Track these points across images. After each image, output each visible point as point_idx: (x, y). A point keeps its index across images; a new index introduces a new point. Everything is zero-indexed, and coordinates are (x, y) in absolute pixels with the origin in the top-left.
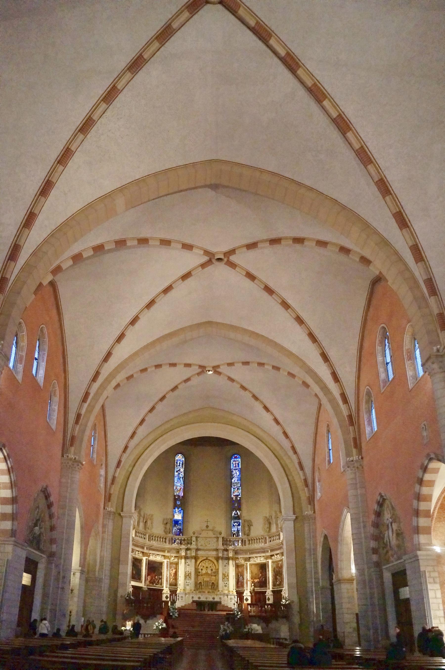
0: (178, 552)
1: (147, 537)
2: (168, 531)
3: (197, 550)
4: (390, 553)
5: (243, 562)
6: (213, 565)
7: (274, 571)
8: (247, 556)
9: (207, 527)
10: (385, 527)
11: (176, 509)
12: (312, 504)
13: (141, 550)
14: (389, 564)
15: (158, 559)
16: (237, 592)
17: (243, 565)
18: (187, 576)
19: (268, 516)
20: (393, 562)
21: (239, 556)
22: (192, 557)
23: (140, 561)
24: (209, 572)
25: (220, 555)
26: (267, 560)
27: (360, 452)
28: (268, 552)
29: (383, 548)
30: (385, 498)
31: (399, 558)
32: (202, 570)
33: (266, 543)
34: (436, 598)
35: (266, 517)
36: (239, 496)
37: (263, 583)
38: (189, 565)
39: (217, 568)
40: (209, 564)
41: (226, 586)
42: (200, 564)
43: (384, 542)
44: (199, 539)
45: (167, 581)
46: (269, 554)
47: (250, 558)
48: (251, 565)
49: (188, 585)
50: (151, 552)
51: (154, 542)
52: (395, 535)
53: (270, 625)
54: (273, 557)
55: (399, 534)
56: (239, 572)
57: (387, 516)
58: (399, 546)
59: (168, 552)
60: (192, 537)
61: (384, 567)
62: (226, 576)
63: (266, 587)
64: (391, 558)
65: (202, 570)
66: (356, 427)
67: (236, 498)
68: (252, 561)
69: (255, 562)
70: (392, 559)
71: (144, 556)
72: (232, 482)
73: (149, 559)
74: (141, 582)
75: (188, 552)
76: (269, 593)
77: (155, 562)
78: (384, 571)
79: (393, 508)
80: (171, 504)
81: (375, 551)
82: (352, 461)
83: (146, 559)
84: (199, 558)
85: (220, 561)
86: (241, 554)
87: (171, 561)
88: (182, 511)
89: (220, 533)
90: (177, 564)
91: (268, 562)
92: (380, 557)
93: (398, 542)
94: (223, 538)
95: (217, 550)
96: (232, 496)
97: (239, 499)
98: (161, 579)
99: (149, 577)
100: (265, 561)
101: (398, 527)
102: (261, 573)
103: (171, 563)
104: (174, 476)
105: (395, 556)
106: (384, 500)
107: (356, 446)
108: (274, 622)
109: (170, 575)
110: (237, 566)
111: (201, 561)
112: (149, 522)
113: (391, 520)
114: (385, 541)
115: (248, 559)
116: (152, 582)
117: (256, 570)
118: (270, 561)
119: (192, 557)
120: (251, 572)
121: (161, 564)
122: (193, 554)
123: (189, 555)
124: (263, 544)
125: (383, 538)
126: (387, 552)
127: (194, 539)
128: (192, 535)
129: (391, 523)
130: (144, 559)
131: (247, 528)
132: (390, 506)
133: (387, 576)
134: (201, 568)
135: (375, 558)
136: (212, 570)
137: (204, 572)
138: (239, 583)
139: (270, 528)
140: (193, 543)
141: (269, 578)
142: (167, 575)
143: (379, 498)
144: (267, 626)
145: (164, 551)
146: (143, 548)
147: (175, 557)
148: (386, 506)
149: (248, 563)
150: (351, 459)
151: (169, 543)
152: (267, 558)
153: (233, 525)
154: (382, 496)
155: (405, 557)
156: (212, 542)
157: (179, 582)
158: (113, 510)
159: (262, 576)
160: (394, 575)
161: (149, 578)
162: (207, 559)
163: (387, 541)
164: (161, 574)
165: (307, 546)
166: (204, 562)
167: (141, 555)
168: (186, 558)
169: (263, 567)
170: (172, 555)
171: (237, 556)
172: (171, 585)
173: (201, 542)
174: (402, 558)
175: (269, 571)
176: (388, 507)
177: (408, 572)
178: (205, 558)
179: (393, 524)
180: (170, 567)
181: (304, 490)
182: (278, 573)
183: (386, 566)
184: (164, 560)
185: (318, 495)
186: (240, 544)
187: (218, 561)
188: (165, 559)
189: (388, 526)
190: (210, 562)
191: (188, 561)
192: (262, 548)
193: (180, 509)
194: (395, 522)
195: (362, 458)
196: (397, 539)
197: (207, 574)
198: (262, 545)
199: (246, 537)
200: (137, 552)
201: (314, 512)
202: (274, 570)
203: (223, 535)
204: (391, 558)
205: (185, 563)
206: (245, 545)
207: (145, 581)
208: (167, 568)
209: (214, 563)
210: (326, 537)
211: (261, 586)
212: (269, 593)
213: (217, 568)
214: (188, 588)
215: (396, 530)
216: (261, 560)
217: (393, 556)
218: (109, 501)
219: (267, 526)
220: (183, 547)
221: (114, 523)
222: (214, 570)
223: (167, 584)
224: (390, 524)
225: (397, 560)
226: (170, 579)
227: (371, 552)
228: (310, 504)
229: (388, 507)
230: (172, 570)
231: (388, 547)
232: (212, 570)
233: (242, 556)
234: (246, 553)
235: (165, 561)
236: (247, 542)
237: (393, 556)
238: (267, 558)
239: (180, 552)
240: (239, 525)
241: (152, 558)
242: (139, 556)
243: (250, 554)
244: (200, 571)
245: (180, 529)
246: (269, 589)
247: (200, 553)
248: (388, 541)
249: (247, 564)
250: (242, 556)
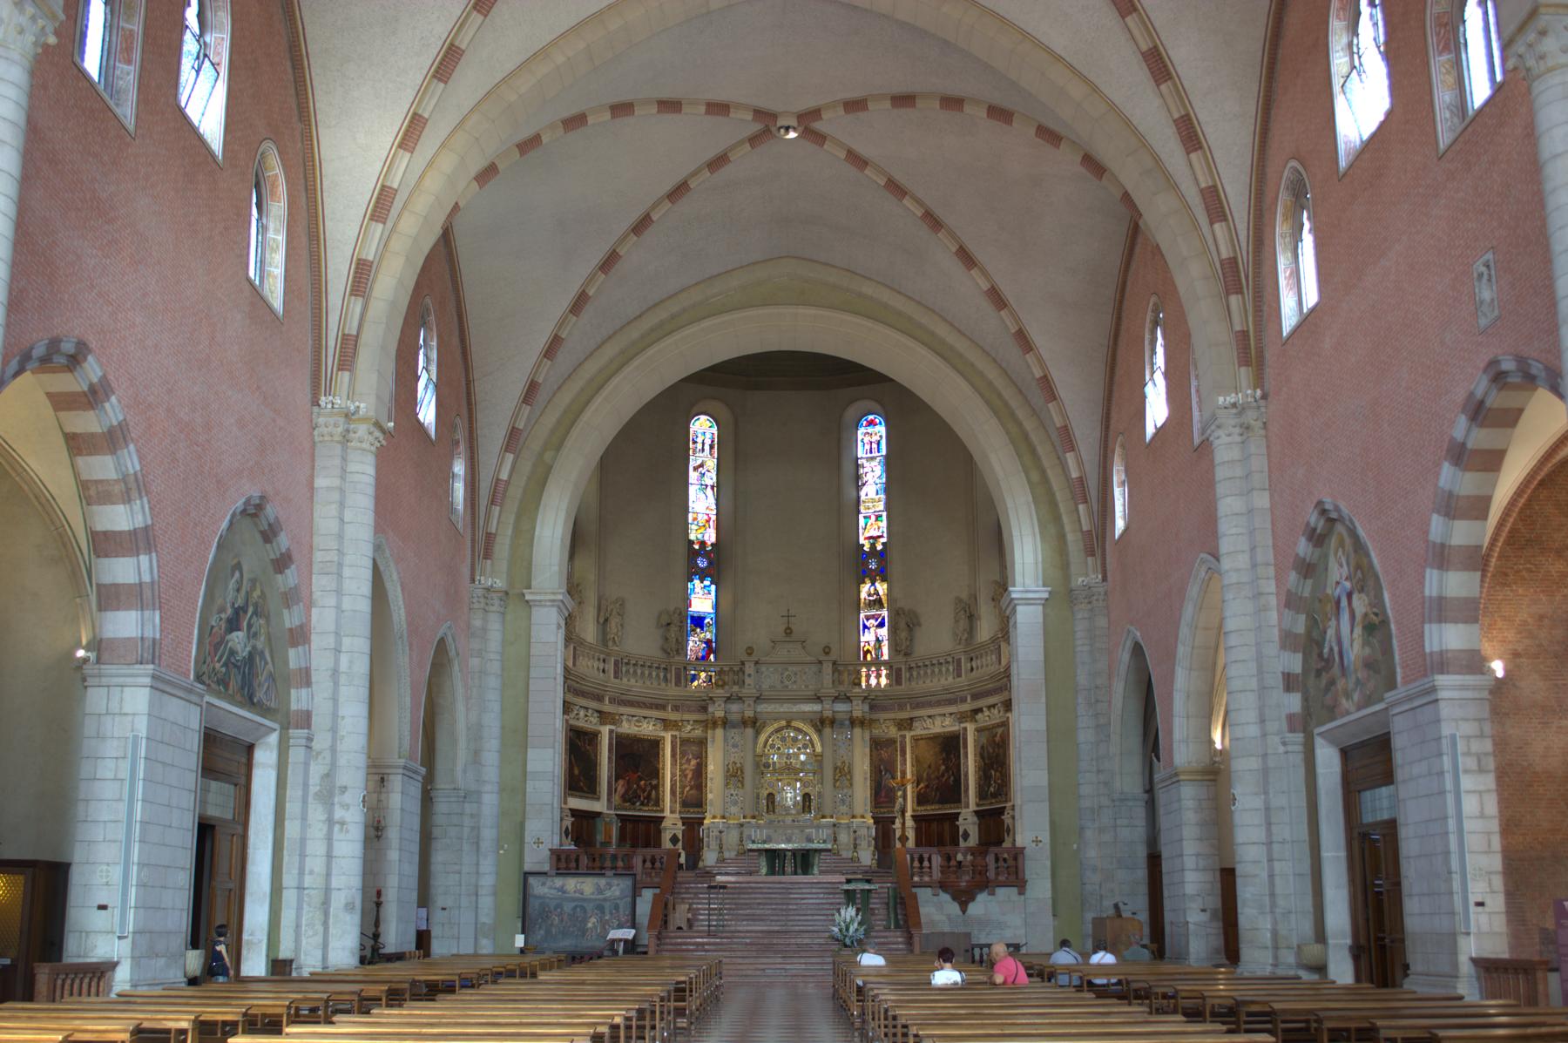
0: (704, 709)
1: (610, 667)
2: (674, 646)
3: (758, 699)
4: (1341, 684)
5: (893, 732)
7: (982, 757)
8: (905, 715)
9: (788, 631)
10: (1329, 608)
11: (697, 582)
12: (1098, 553)
13: (593, 705)
14: (1333, 719)
15: (648, 729)
16: (877, 821)
17: (893, 741)
18: (734, 775)
19: (964, 595)
20: (1348, 713)
21: (882, 716)
22: (744, 723)
23: (593, 737)
25: (828, 714)
27: (1259, 381)
28: (964, 700)
29: (1319, 673)
30: (1334, 515)
31: (1368, 701)
33: (959, 675)
34: (1482, 816)
35: (959, 600)
37: (951, 791)
38: (734, 746)
41: (843, 801)
43: (1320, 655)
44: (763, 669)
45: (673, 792)
46: (966, 707)
47: (911, 719)
48: (916, 740)
49: (735, 803)
50: (622, 710)
51: (633, 681)
52: (1358, 631)
53: (976, 908)
54: (979, 716)
55: (1375, 627)
56: (881, 760)
57: (1338, 572)
58: (1369, 665)
59: (676, 708)
60: (743, 663)
61: (1317, 731)
62: (843, 774)
63: (959, 801)
64: (1344, 701)
66: (1249, 295)
67: (873, 546)
68: (919, 730)
70: (1345, 704)
71: (603, 723)
72: (859, 497)
73: (620, 730)
74: (598, 799)
75: (735, 707)
76: (967, 821)
77: (636, 740)
78: (1319, 742)
79: (1359, 547)
80: (680, 566)
81: (1290, 683)
82: (1234, 405)
83: (611, 732)
84: (764, 725)
85: (827, 731)
86: (884, 709)
87: (684, 735)
88: (713, 587)
89: (827, 651)
90: (702, 743)
92: (1306, 699)
93: (1367, 651)
94: (834, 663)
95: (818, 699)
96: (862, 541)
98: (656, 787)
99: (621, 782)
100: (956, 728)
101: (1371, 605)
102: (945, 761)
103: (685, 742)
104: (686, 484)
105: (1356, 696)
106: (1331, 521)
107: (1245, 360)
108: (982, 897)
109: (683, 775)
110: (877, 744)
112: (614, 622)
113: (1348, 585)
114: (1326, 650)
115: (907, 724)
116: (630, 798)
117: (930, 754)
118: (970, 728)
119: (744, 723)
120: (917, 761)
121: (655, 744)
122: (749, 714)
123: (735, 717)
124: (950, 679)
125: (1320, 645)
126: (1332, 682)
127: (749, 668)
128: (745, 658)
129: (1349, 596)
130: (605, 730)
131: (903, 635)
132: (1348, 541)
133: (1328, 761)
135: (1294, 702)
138: (882, 795)
139: (971, 631)
140: (748, 681)
142: (673, 775)
143: (1314, 519)
144: (964, 912)
145: (662, 707)
146: (600, 699)
148: (1334, 541)
149: (908, 735)
150: (1231, 399)
151: (678, 683)
152: (962, 718)
153: (865, 627)
154: (1324, 512)
155: (1390, 696)
157: (710, 796)
158: (500, 583)
159: (947, 769)
160: (1345, 753)
161: (621, 787)
162: (788, 726)
163: (1331, 649)
164: (655, 773)
165: (1082, 679)
167: (594, 720)
168: (725, 723)
169: (950, 745)
170: (686, 717)
171: (875, 716)
172: (685, 804)
173: (770, 679)
174: (1381, 700)
176: (1341, 544)
177: (1398, 742)
178: (783, 723)
179: (1355, 597)
180: (683, 754)
181: (1077, 510)
182: (996, 760)
183: (1323, 729)
185: (1120, 524)
186: (884, 681)
187: (819, 731)
188: (666, 728)
189: (1338, 602)
191: (732, 732)
192: (947, 690)
193: (707, 583)
194: (1361, 590)
195: (1264, 397)
196: (1365, 643)
198: (947, 680)
199: (901, 658)
200: (582, 713)
201: (1104, 579)
202: (982, 753)
203: (833, 656)
204: (1344, 701)
205: (726, 740)
206: (898, 682)
207: (610, 794)
208: (673, 755)
210: (1137, 650)
211: (943, 801)
212: (967, 821)
213: (819, 749)
214: (734, 809)
215: (1366, 615)
216: (943, 725)
217: (1348, 696)
218: (488, 555)
219: (963, 623)
220: (720, 691)
221: (503, 622)
223: (673, 801)
224: (1344, 602)
225: (1359, 709)
226: (683, 787)
227: (1279, 682)
228: (1090, 552)
229: (1341, 544)
230: (688, 761)
231: (1336, 670)
233: (892, 716)
234: (901, 707)
235: (668, 736)
236: (905, 675)
237: (1348, 696)
239: (711, 709)
240: (881, 625)
241: (627, 728)
242: (588, 722)
243: (912, 709)
245: (708, 642)
246: (967, 806)
247: (763, 708)
248: (1336, 649)
249: (904, 737)
250: (892, 716)
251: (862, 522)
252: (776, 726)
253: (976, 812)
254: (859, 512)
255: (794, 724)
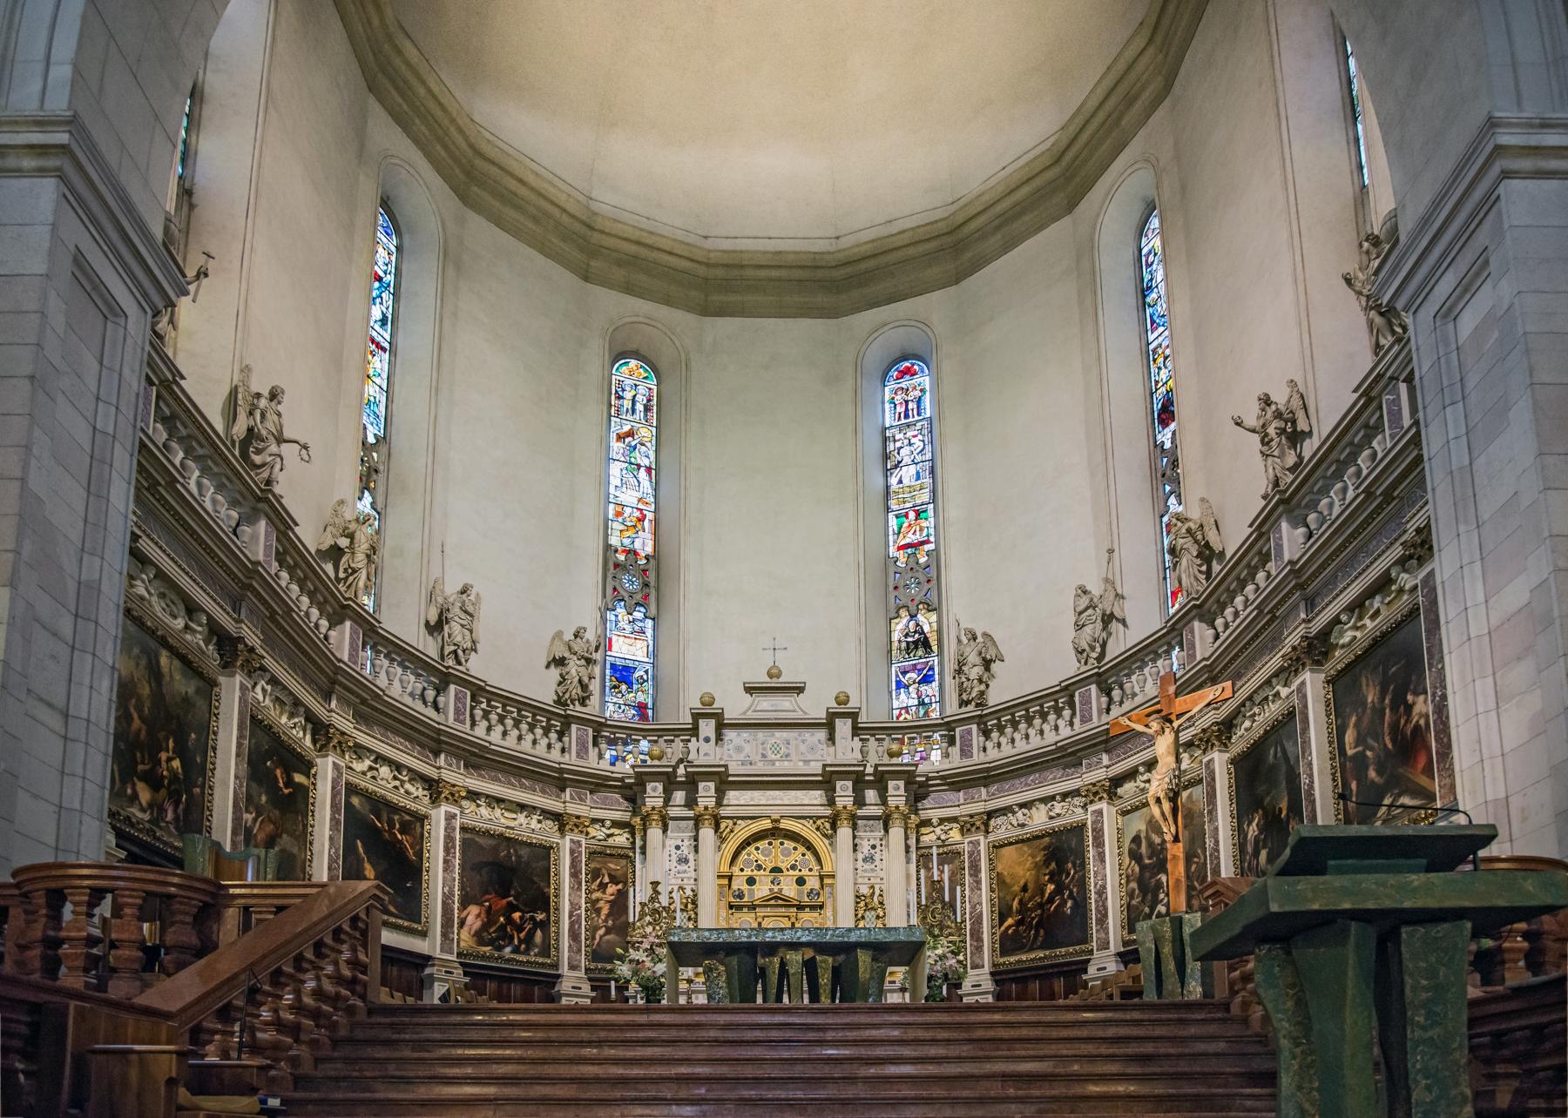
6: (809, 855)
7: (1135, 855)
15: (527, 827)
23: (415, 822)
24: (789, 890)
26: (1091, 808)
32: (751, 881)
36: (927, 547)
39: (827, 868)
40: (786, 854)
42: (743, 856)
65: (751, 881)
69: (1020, 832)
83: (450, 817)
85: (844, 832)
91: (1100, 813)
96: (892, 551)
97: (923, 560)
111: (747, 843)
134: (748, 872)
136: (801, 881)
137: (762, 890)
141: (1101, 892)
147: (616, 824)
152: (1092, 794)
156: (803, 748)
166: (763, 844)
175: (1101, 857)
178: (766, 824)
184: (555, 839)
190: (789, 844)
197: (778, 900)
200: (385, 771)
209: (810, 847)
213: (827, 868)
222: (813, 883)
230: (603, 887)
232: (801, 881)
238: (1092, 794)
241: (484, 816)
244: (745, 887)
251: (893, 522)
252: (756, 827)
253: (1119, 954)
254: (888, 509)
255: (786, 824)
